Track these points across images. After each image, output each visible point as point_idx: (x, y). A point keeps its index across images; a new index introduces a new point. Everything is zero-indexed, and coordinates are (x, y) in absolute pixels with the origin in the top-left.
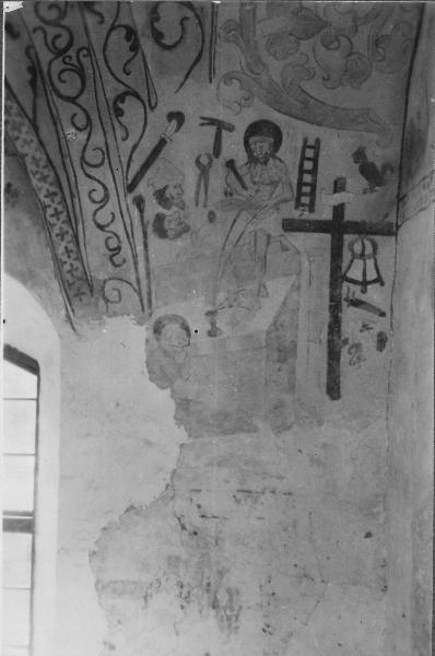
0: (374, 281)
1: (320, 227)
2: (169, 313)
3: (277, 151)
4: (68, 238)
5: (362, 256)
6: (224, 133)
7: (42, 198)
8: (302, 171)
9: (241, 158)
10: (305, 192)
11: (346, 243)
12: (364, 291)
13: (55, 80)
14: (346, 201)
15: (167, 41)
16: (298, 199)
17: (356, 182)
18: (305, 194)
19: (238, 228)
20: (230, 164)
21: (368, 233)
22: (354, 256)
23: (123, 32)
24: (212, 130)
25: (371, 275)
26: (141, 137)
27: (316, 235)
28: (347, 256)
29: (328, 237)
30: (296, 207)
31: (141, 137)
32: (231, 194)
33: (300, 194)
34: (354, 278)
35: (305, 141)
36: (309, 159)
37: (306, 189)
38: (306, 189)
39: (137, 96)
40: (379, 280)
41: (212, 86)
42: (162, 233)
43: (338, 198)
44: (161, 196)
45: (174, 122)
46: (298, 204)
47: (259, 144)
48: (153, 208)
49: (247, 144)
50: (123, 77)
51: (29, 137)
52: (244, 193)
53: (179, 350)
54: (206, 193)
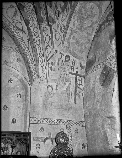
0: (81, 85)
1: (74, 74)
3: (69, 60)
4: (34, 68)
5: (80, 80)
7: (29, 61)
9: (64, 61)
10: (72, 68)
13: (36, 41)
15: (57, 39)
16: (71, 69)
17: (80, 68)
19: (62, 72)
20: (62, 61)
21: (81, 76)
24: (61, 54)
28: (77, 80)
29: (75, 76)
33: (72, 68)
35: (73, 60)
38: (73, 68)
43: (77, 70)
44: (52, 63)
46: (71, 70)
48: (51, 65)
49: (65, 58)
50: (48, 43)
51: (27, 50)
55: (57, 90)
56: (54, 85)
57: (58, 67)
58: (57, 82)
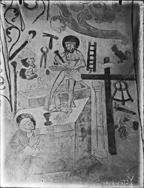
0: (128, 100)
2: (25, 113)
3: (77, 47)
5: (121, 89)
6: (54, 40)
8: (89, 56)
9: (62, 50)
11: (112, 84)
12: (124, 104)
14: (110, 66)
18: (91, 64)
19: (60, 78)
20: (57, 52)
21: (122, 79)
22: (116, 89)
23: (13, 10)
24: (49, 38)
25: (126, 97)
26: (17, 41)
27: (98, 81)
28: (113, 90)
29: (103, 81)
30: (87, 70)
31: (17, 41)
32: (57, 64)
33: (89, 64)
34: (118, 98)
35: (90, 43)
36: (92, 51)
37: (92, 62)
39: (17, 28)
40: (130, 99)
41: (48, 22)
42: (24, 77)
43: (107, 65)
44: (24, 62)
45: (32, 34)
46: (88, 68)
47: (69, 45)
49: (64, 45)
52: (63, 64)
53: (29, 131)
54: (45, 62)
55: (48, 123)
56: (38, 113)
57: (45, 67)
58: (46, 104)
